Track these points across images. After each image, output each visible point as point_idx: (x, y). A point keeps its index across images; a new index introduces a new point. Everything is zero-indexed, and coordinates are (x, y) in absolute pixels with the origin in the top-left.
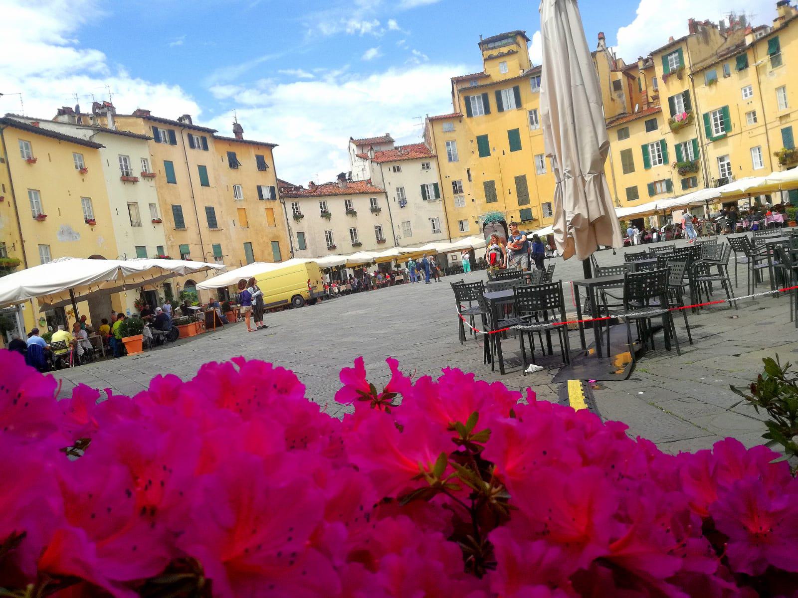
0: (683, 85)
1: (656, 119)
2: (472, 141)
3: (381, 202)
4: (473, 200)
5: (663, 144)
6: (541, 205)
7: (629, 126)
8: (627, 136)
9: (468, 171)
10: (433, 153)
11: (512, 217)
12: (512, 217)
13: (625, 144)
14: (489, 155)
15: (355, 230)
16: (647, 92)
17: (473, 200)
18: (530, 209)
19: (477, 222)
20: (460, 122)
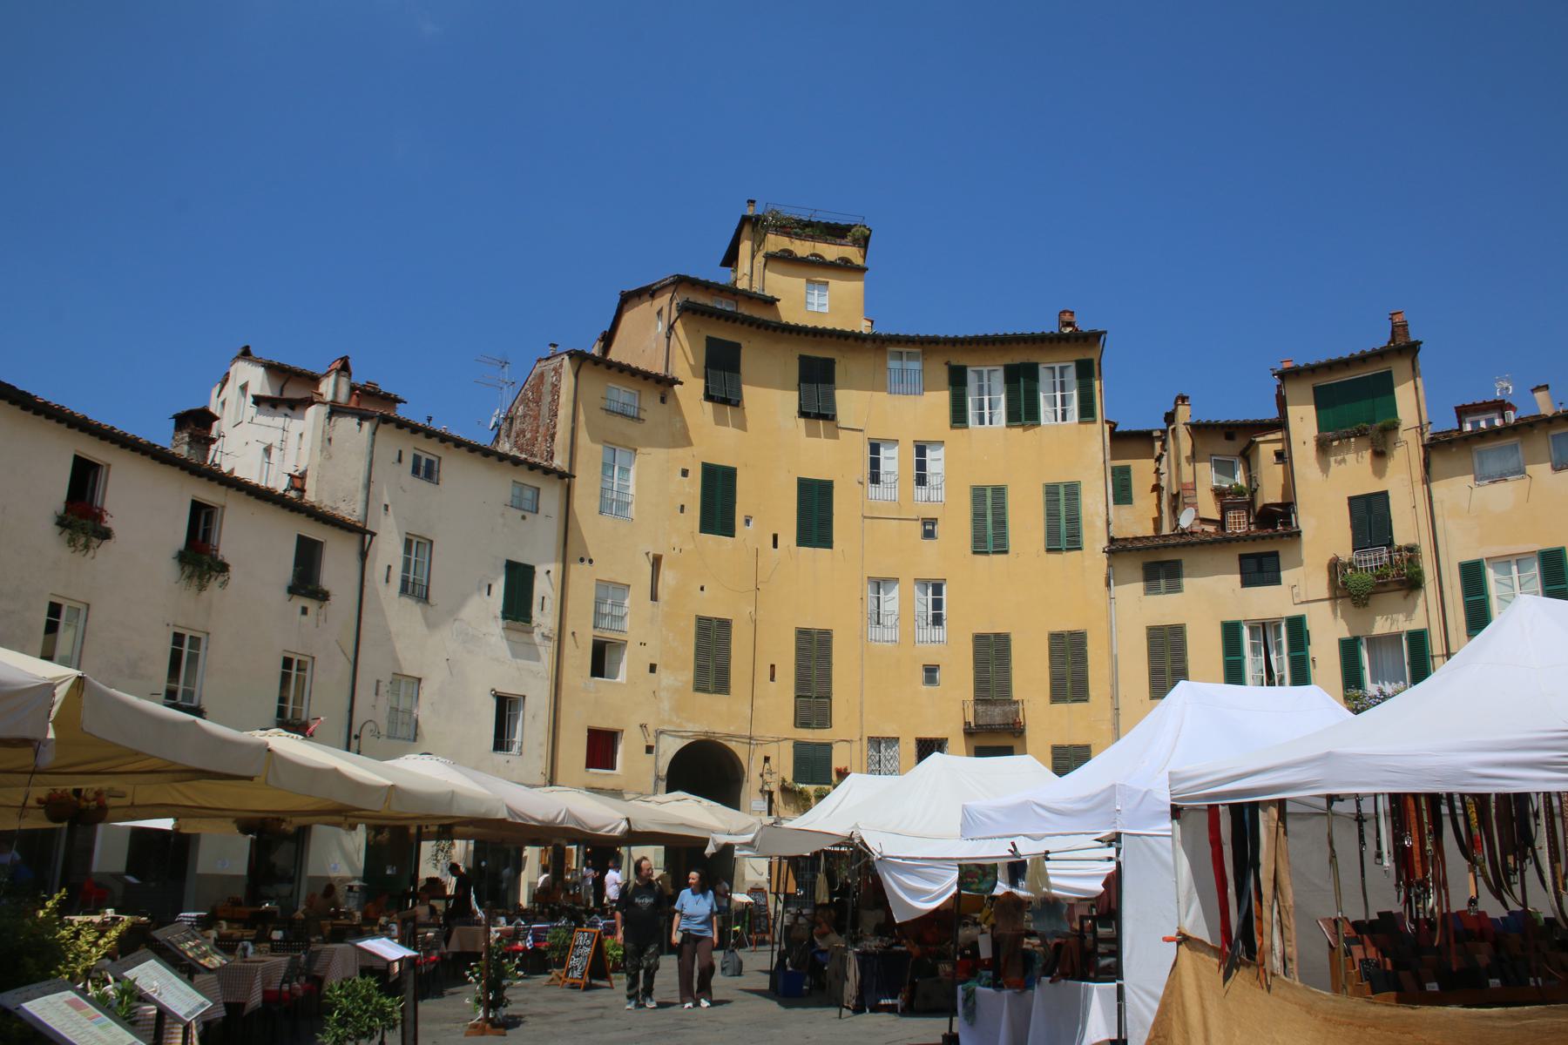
0: (1379, 472)
1: (1276, 554)
2: (685, 473)
3: (336, 567)
4: (653, 668)
5: (1297, 629)
6: (865, 741)
7: (1186, 558)
8: (1177, 589)
9: (657, 561)
10: (559, 462)
11: (767, 759)
12: (767, 759)
13: (1165, 608)
14: (732, 535)
15: (195, 642)
16: (1195, 490)
17: (653, 668)
18: (828, 747)
19: (649, 749)
20: (663, 400)
